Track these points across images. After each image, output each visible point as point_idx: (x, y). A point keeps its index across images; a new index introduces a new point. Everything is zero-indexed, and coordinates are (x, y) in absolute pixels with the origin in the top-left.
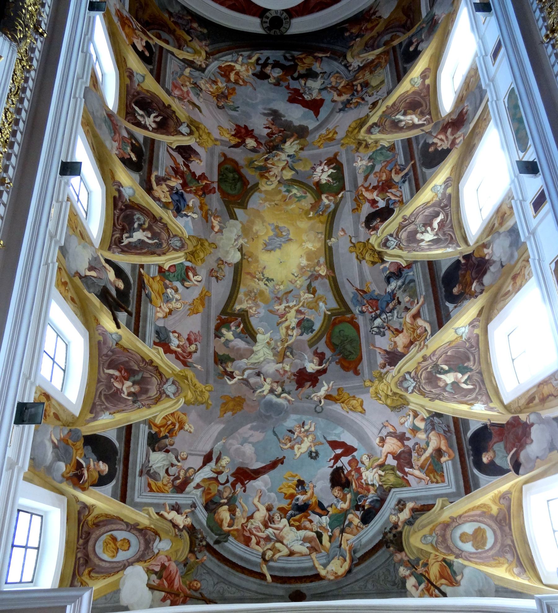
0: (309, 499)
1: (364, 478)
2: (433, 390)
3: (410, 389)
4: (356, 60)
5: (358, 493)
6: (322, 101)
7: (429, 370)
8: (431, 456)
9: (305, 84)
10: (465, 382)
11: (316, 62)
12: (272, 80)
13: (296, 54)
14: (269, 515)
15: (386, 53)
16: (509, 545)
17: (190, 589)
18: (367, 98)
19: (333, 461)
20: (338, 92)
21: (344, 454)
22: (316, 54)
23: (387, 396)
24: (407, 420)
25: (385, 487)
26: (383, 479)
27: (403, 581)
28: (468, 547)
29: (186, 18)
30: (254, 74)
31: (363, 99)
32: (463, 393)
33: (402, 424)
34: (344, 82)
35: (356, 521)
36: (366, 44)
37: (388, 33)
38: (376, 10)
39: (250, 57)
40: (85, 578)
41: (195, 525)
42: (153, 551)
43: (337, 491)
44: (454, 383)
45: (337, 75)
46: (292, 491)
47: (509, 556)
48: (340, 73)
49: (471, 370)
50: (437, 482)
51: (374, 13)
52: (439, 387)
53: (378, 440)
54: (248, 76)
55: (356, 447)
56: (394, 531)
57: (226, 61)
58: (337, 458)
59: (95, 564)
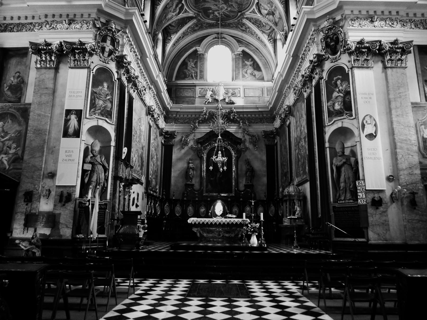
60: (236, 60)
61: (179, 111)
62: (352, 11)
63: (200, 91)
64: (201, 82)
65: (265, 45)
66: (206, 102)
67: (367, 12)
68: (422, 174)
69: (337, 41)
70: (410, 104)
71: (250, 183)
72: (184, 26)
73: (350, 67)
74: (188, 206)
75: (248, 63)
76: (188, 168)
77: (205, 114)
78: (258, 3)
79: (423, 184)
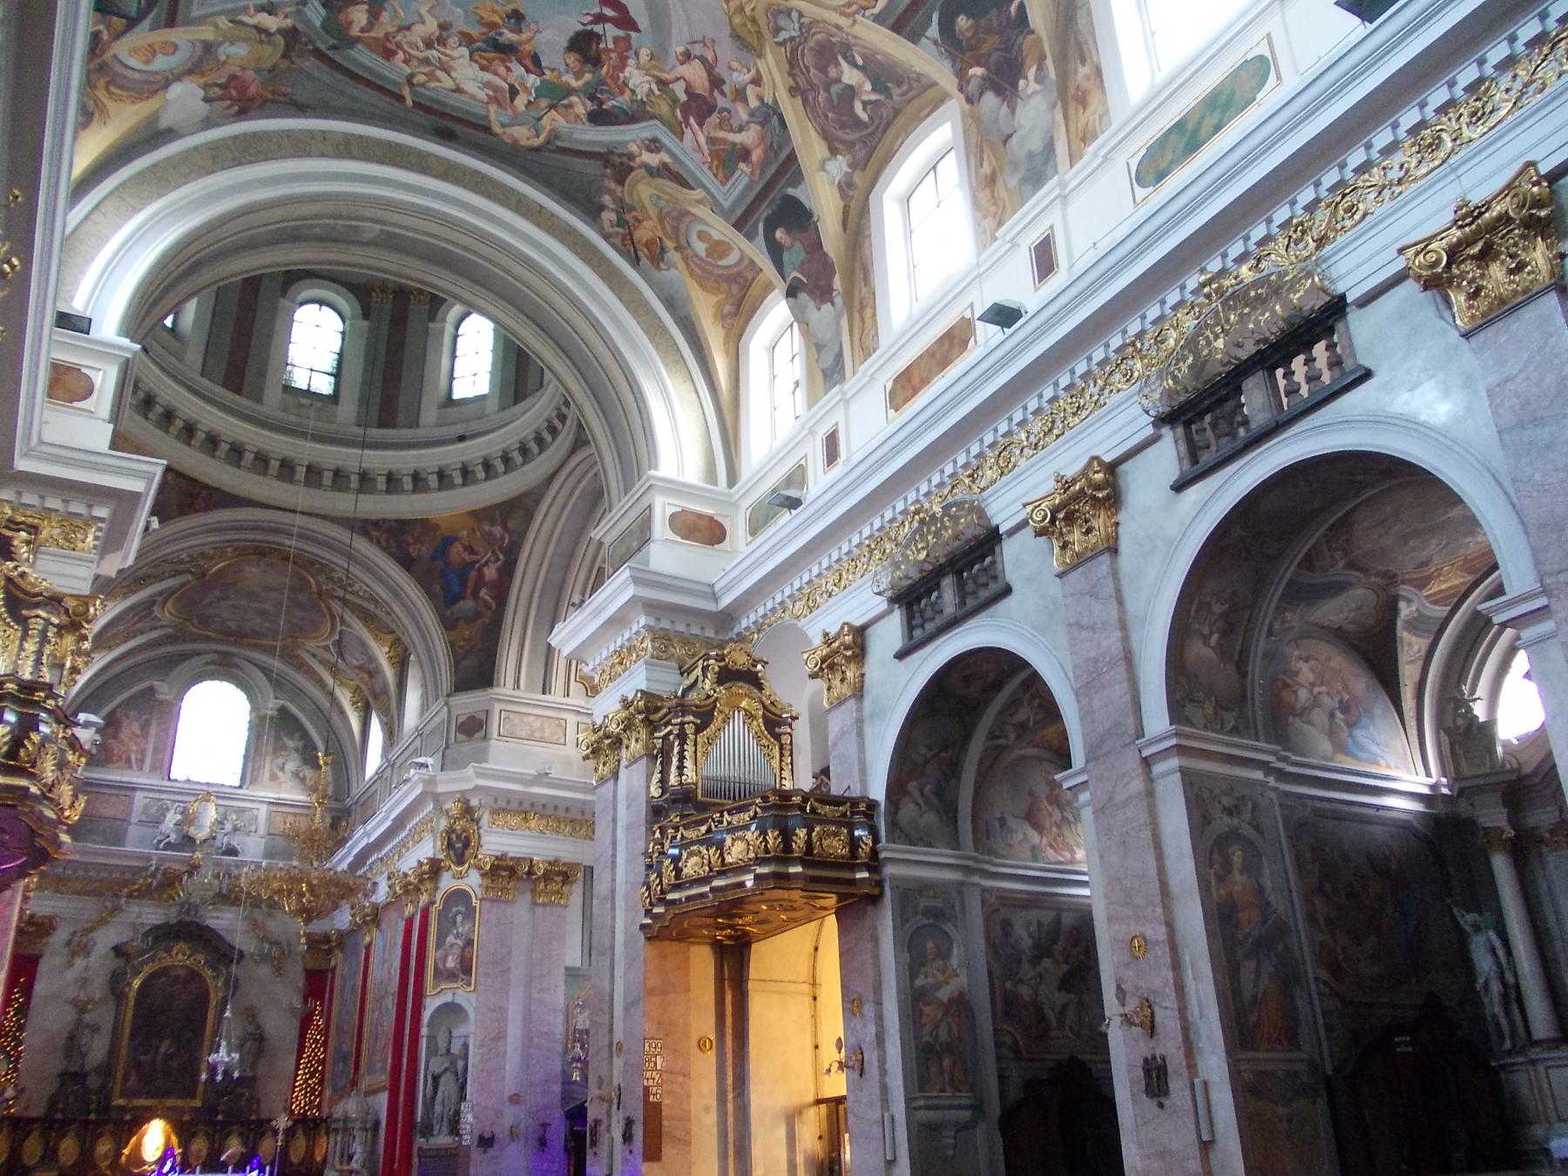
0: (521, 43)
1: (627, 73)
2: (812, 70)
3: (783, 36)
5: (605, 83)
7: (834, 39)
8: (734, 144)
10: (865, 103)
14: (441, 35)
16: (746, 280)
17: (274, 92)
19: (590, 18)
21: (618, 23)
23: (741, 9)
24: (740, 72)
25: (648, 108)
26: (653, 99)
27: (602, 208)
28: (700, 248)
32: (845, 119)
33: (730, 68)
35: (580, 110)
40: (101, 94)
41: (300, 27)
42: (216, 57)
43: (572, 59)
44: (850, 88)
46: (496, 19)
47: (735, 288)
49: (890, 97)
50: (716, 176)
52: (825, 73)
53: (680, 49)
55: (641, 26)
56: (625, 159)
58: (600, 19)
59: (116, 74)
60: (257, 728)
61: (75, 861)
62: (496, 800)
63: (146, 807)
64: (155, 781)
65: (342, 712)
66: (160, 842)
67: (521, 803)
68: (563, 1092)
69: (467, 844)
70: (563, 971)
71: (249, 1074)
72: (135, 636)
73: (480, 896)
74: (64, 1136)
75: (291, 744)
76: (79, 1025)
77: (153, 875)
78: (339, 643)
79: (562, 1107)
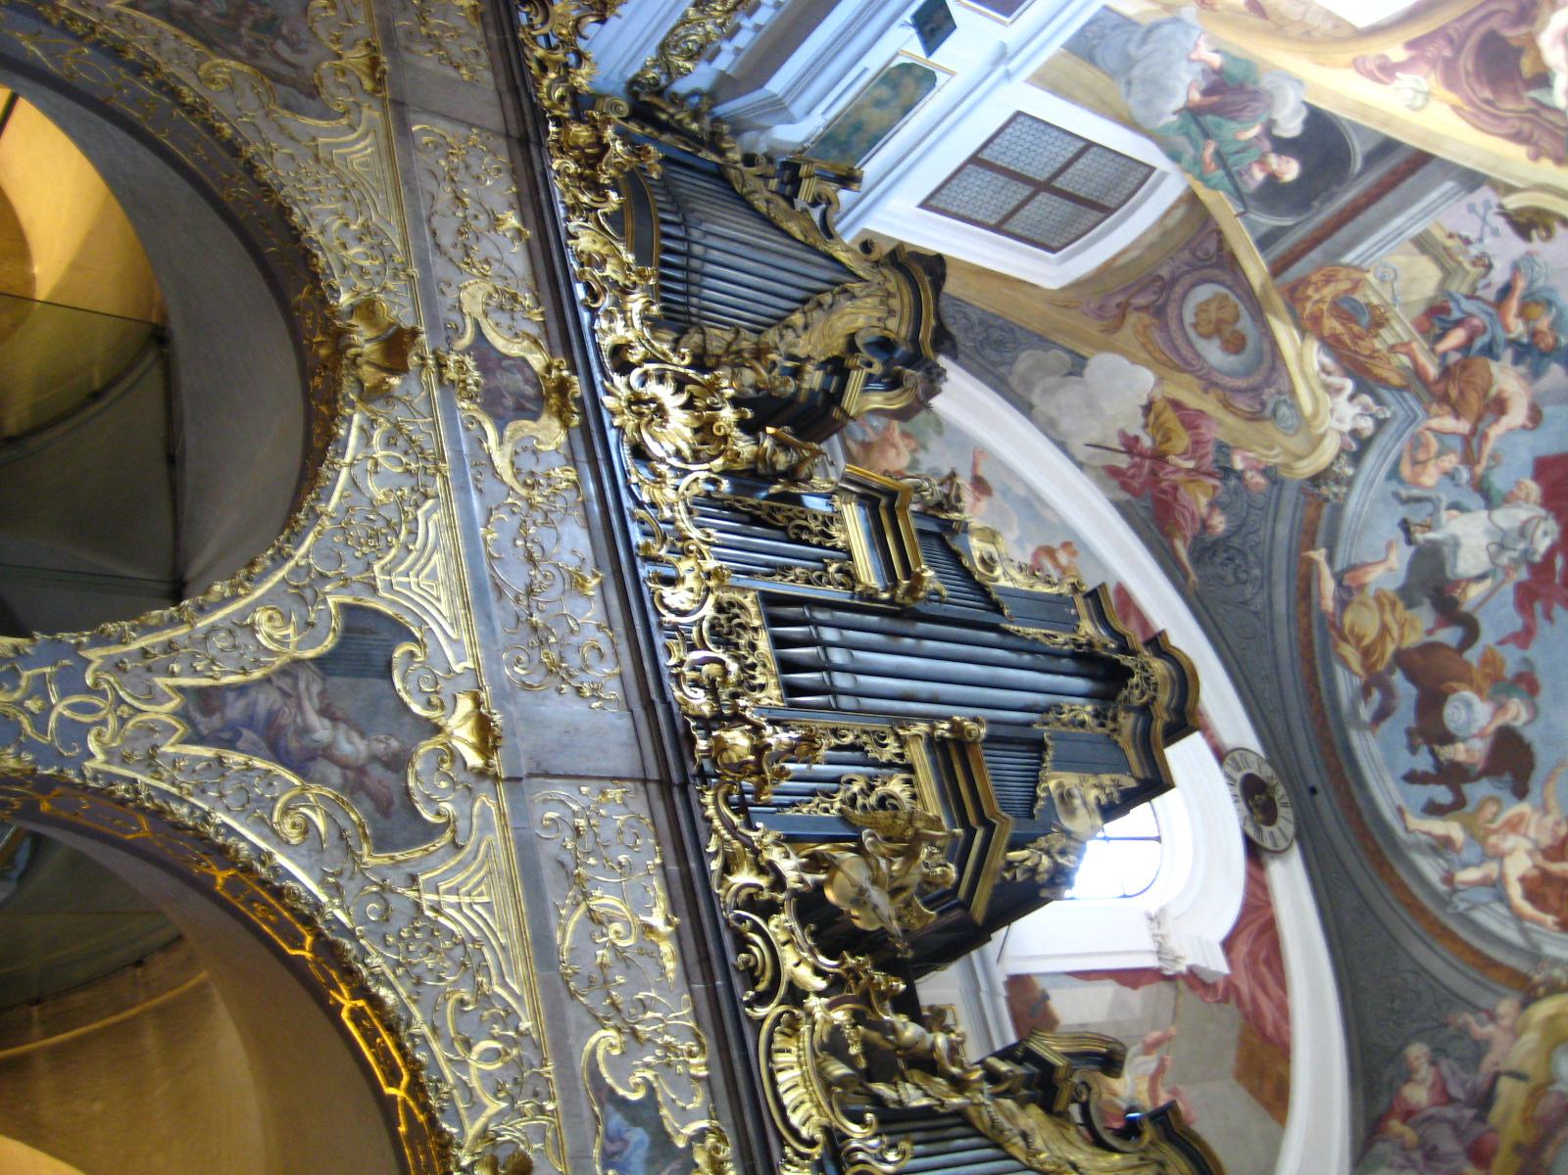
4: (1330, 422)
6: (1543, 468)
9: (1482, 577)
11: (1362, 587)
12: (1516, 712)
13: (1346, 684)
15: (1294, 296)
18: (1499, 276)
20: (1489, 417)
22: (1329, 604)
29: (1410, 1135)
30: (1521, 792)
31: (1506, 291)
34: (1435, 423)
36: (1254, 417)
37: (1198, 355)
38: (1116, 443)
39: (1442, 846)
45: (1406, 470)
48: (1397, 463)
51: (1130, 445)
54: (1544, 809)
57: (1518, 917)
